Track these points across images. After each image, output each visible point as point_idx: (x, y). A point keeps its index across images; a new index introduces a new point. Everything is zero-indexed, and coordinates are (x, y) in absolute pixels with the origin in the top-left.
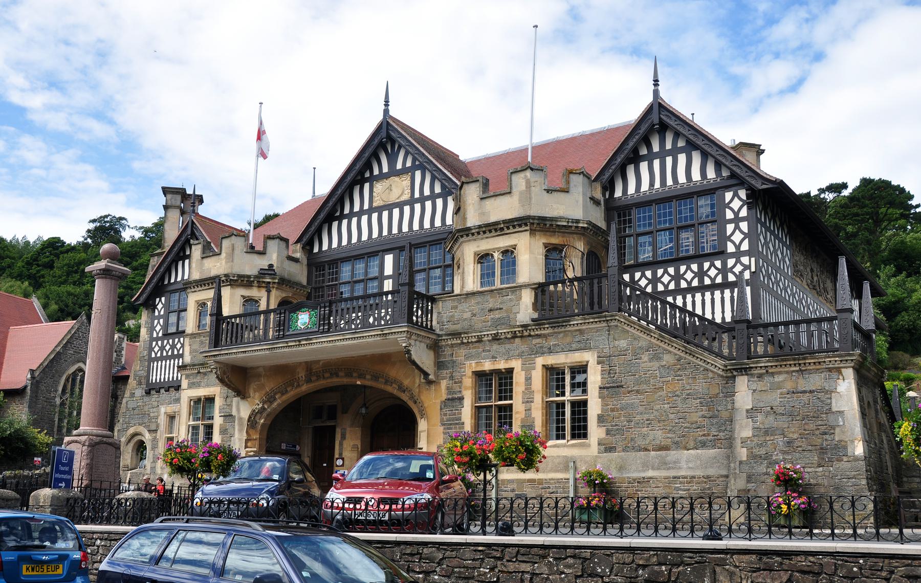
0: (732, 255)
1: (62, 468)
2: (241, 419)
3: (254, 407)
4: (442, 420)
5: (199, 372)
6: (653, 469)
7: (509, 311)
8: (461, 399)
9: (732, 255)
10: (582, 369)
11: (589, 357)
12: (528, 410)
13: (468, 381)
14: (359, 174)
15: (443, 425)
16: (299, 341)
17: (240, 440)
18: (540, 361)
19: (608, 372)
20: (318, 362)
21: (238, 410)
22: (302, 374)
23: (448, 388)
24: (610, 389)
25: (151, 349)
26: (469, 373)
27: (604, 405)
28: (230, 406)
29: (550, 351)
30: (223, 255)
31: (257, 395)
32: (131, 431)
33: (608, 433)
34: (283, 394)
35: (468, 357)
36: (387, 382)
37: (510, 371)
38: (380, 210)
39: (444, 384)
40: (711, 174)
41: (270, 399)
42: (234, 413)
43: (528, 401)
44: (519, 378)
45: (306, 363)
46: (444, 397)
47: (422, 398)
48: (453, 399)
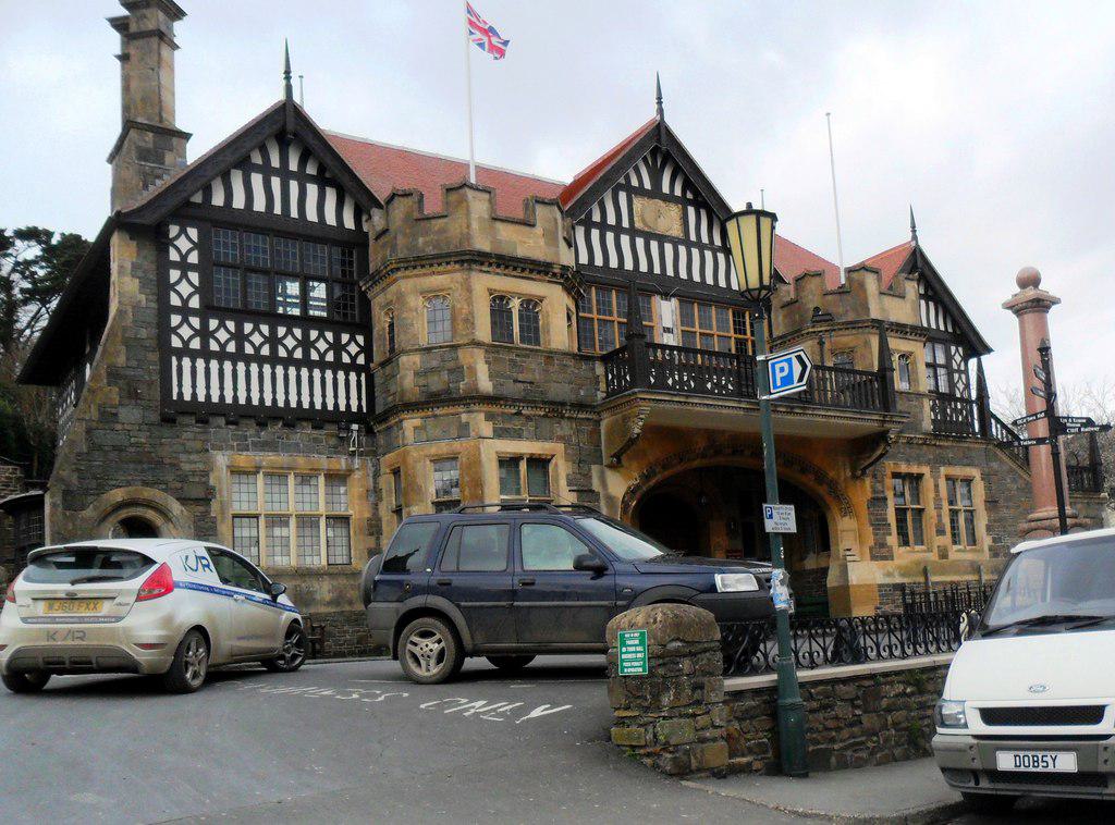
2: (610, 499)
3: (631, 483)
4: (870, 521)
5: (519, 414)
7: (914, 416)
10: (968, 481)
11: (975, 473)
12: (939, 516)
14: (607, 177)
15: (872, 525)
16: (793, 408)
19: (988, 488)
20: (724, 432)
21: (604, 483)
22: (701, 444)
24: (991, 503)
25: (165, 331)
27: (989, 517)
28: (588, 476)
29: (950, 464)
30: (538, 230)
31: (635, 465)
32: (118, 495)
34: (665, 467)
36: (803, 471)
37: (920, 477)
39: (868, 482)
41: (646, 478)
42: (596, 485)
43: (938, 507)
44: (928, 482)
45: (707, 431)
46: (869, 495)
47: (850, 494)
48: (878, 499)
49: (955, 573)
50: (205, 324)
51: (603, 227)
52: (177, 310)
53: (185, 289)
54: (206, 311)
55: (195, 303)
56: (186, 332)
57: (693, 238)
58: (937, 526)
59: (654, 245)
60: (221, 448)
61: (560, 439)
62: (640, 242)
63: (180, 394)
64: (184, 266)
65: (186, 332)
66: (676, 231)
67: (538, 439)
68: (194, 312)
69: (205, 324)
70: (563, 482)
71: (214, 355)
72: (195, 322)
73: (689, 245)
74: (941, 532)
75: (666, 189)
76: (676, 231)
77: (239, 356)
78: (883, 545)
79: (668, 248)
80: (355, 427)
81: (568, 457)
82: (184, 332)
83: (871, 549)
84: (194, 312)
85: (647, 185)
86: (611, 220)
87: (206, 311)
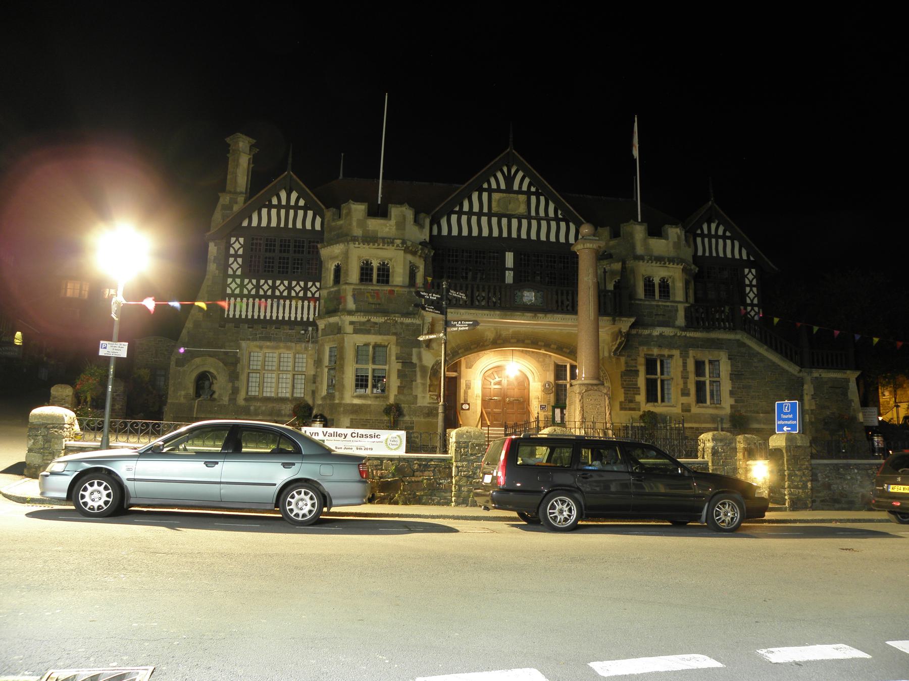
0: (749, 305)
1: (785, 417)
2: (424, 369)
4: (622, 384)
6: (764, 424)
8: (637, 372)
9: (749, 305)
13: (641, 360)
17: (424, 384)
18: (691, 353)
21: (420, 358)
23: (626, 363)
26: (642, 354)
33: (736, 401)
35: (642, 344)
38: (500, 216)
40: (745, 257)
42: (415, 360)
46: (623, 368)
49: (695, 422)
50: (242, 282)
51: (470, 213)
52: (230, 276)
53: (235, 266)
54: (242, 277)
55: (239, 272)
56: (233, 286)
57: (533, 213)
58: (682, 390)
59: (504, 221)
60: (244, 340)
61: (395, 334)
62: (494, 220)
63: (228, 315)
64: (236, 256)
65: (233, 286)
66: (522, 209)
67: (380, 334)
68: (238, 277)
69: (242, 282)
70: (393, 358)
71: (245, 296)
72: (238, 281)
73: (529, 218)
74: (685, 393)
75: (516, 187)
76: (522, 209)
77: (258, 295)
78: (631, 401)
79: (515, 222)
80: (310, 329)
81: (397, 344)
82: (233, 286)
83: (621, 403)
84: (238, 277)
85: (503, 186)
86: (476, 209)
87: (242, 277)
